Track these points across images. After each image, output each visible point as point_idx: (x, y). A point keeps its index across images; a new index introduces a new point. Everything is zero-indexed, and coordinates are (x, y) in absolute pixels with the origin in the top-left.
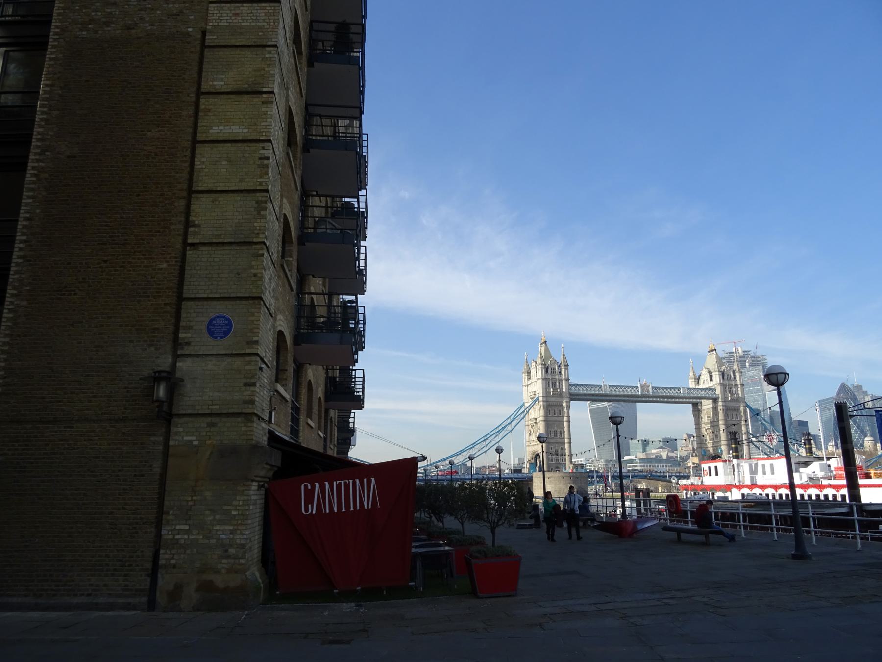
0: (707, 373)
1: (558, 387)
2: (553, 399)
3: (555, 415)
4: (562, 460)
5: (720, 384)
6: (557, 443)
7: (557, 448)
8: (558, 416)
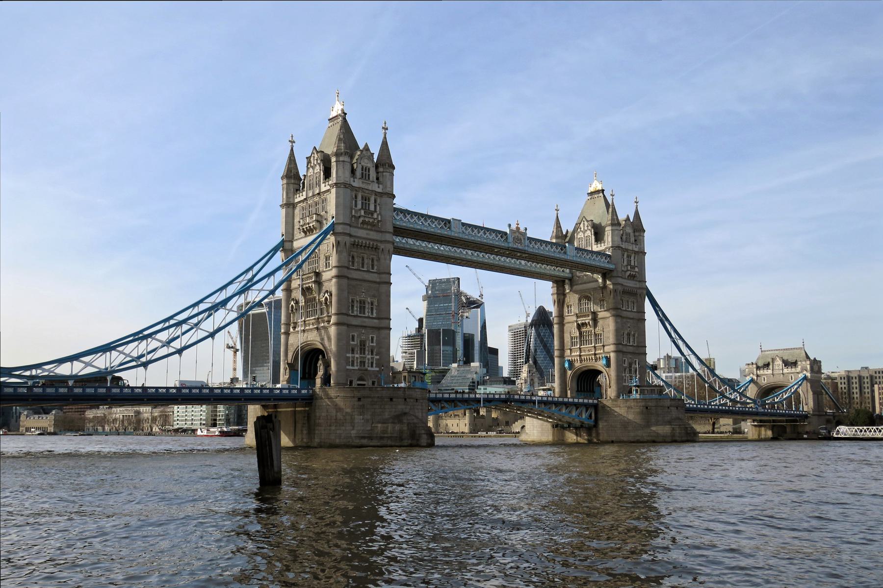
0: (590, 228)
1: (372, 208)
2: (362, 233)
3: (363, 267)
4: (372, 363)
5: (612, 247)
6: (365, 327)
7: (363, 337)
8: (368, 271)
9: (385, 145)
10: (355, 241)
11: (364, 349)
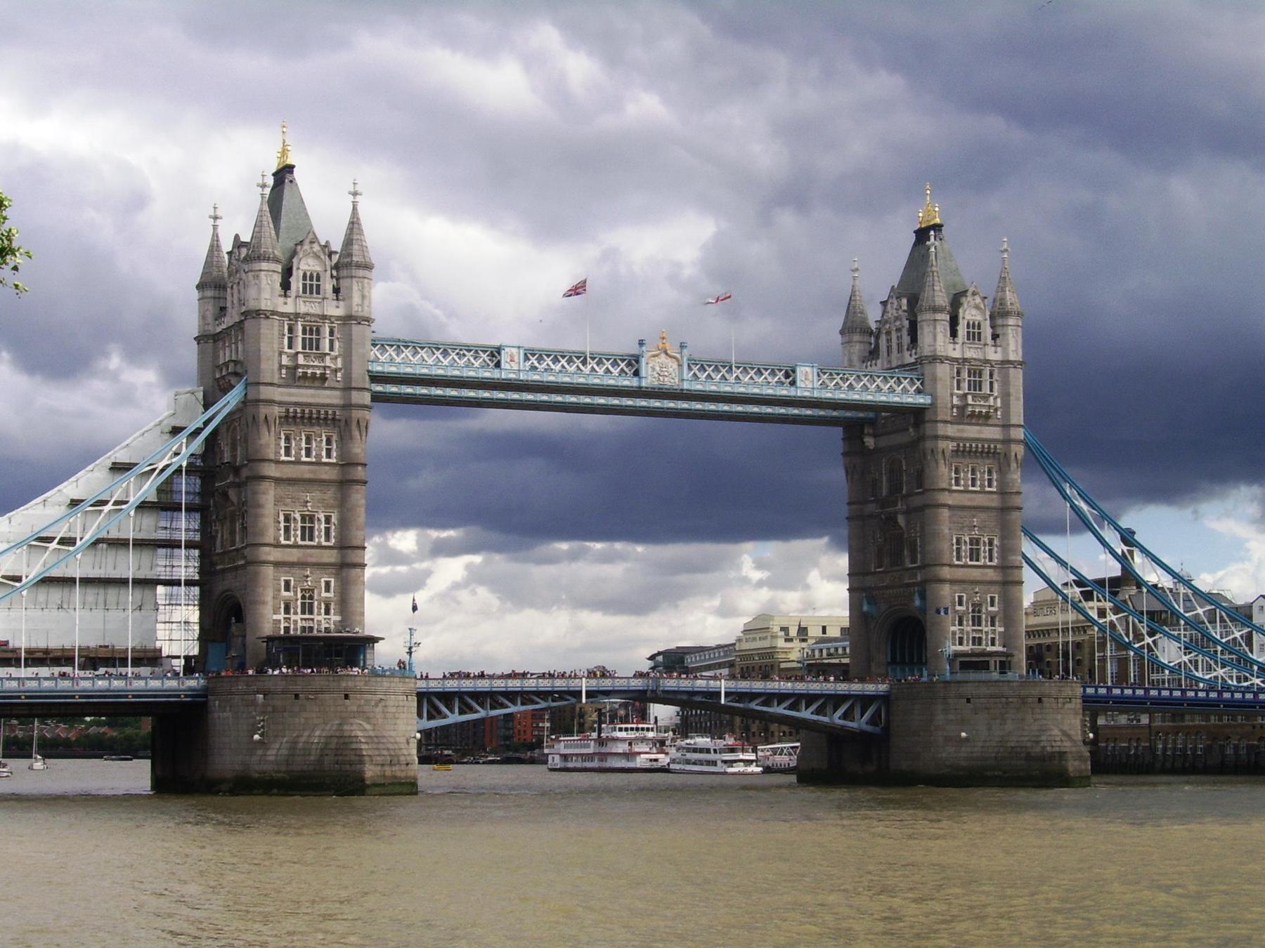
9: (354, 224)
10: (287, 411)
11: (311, 605)
